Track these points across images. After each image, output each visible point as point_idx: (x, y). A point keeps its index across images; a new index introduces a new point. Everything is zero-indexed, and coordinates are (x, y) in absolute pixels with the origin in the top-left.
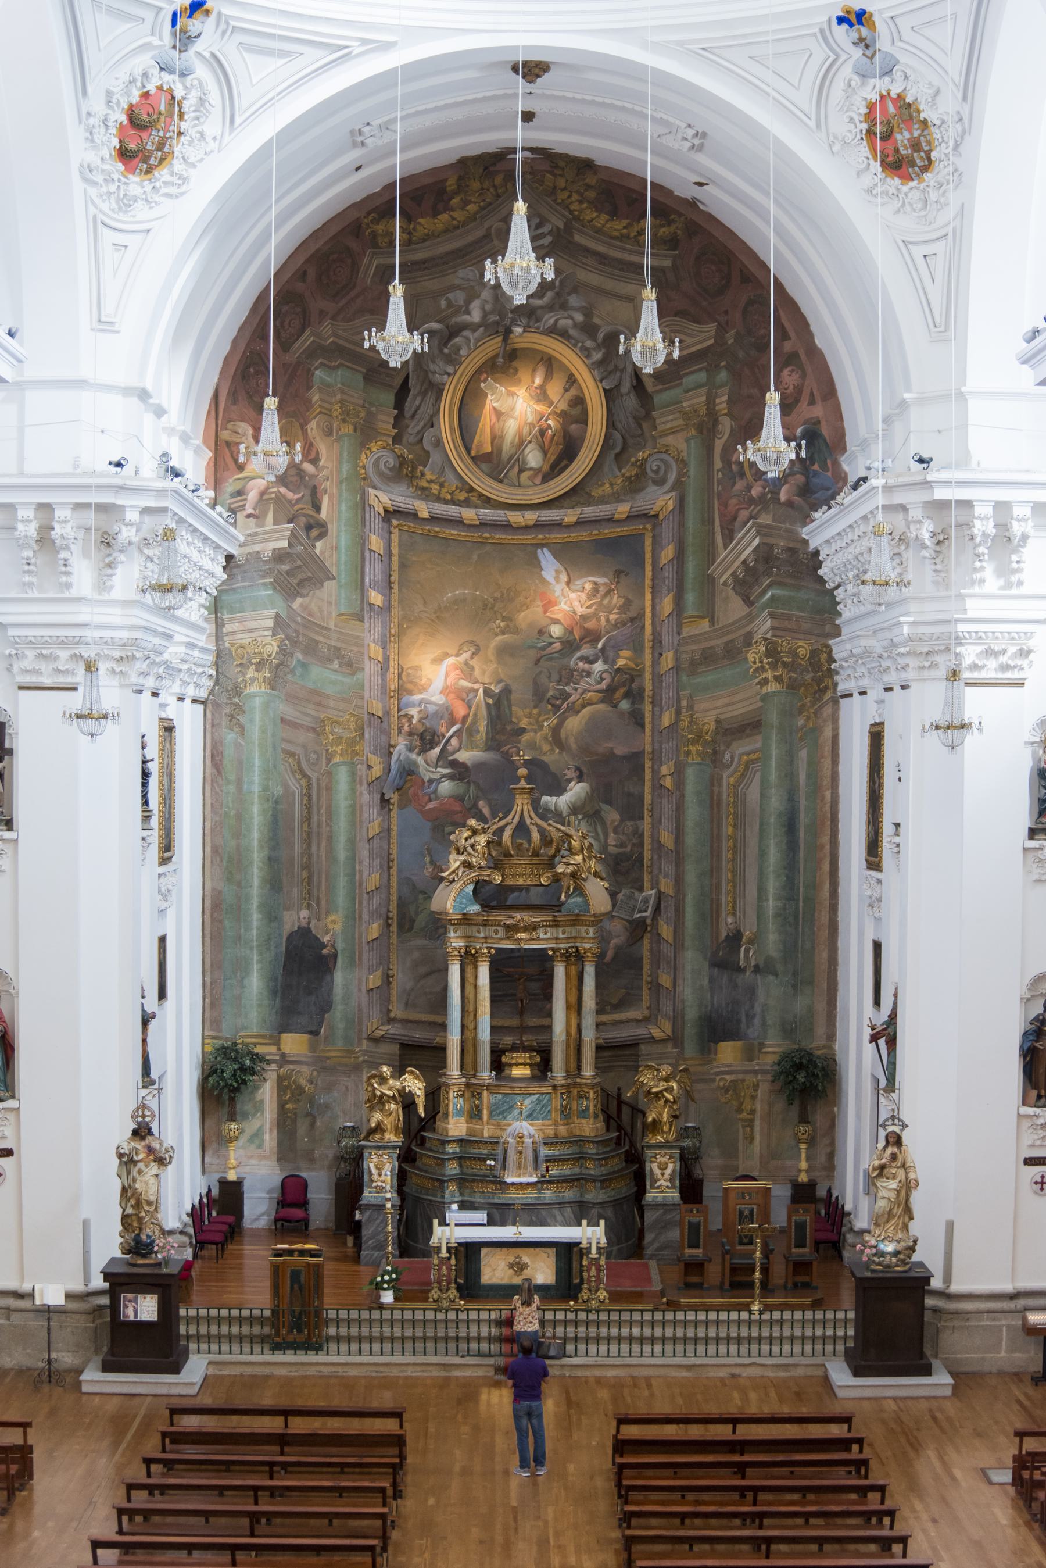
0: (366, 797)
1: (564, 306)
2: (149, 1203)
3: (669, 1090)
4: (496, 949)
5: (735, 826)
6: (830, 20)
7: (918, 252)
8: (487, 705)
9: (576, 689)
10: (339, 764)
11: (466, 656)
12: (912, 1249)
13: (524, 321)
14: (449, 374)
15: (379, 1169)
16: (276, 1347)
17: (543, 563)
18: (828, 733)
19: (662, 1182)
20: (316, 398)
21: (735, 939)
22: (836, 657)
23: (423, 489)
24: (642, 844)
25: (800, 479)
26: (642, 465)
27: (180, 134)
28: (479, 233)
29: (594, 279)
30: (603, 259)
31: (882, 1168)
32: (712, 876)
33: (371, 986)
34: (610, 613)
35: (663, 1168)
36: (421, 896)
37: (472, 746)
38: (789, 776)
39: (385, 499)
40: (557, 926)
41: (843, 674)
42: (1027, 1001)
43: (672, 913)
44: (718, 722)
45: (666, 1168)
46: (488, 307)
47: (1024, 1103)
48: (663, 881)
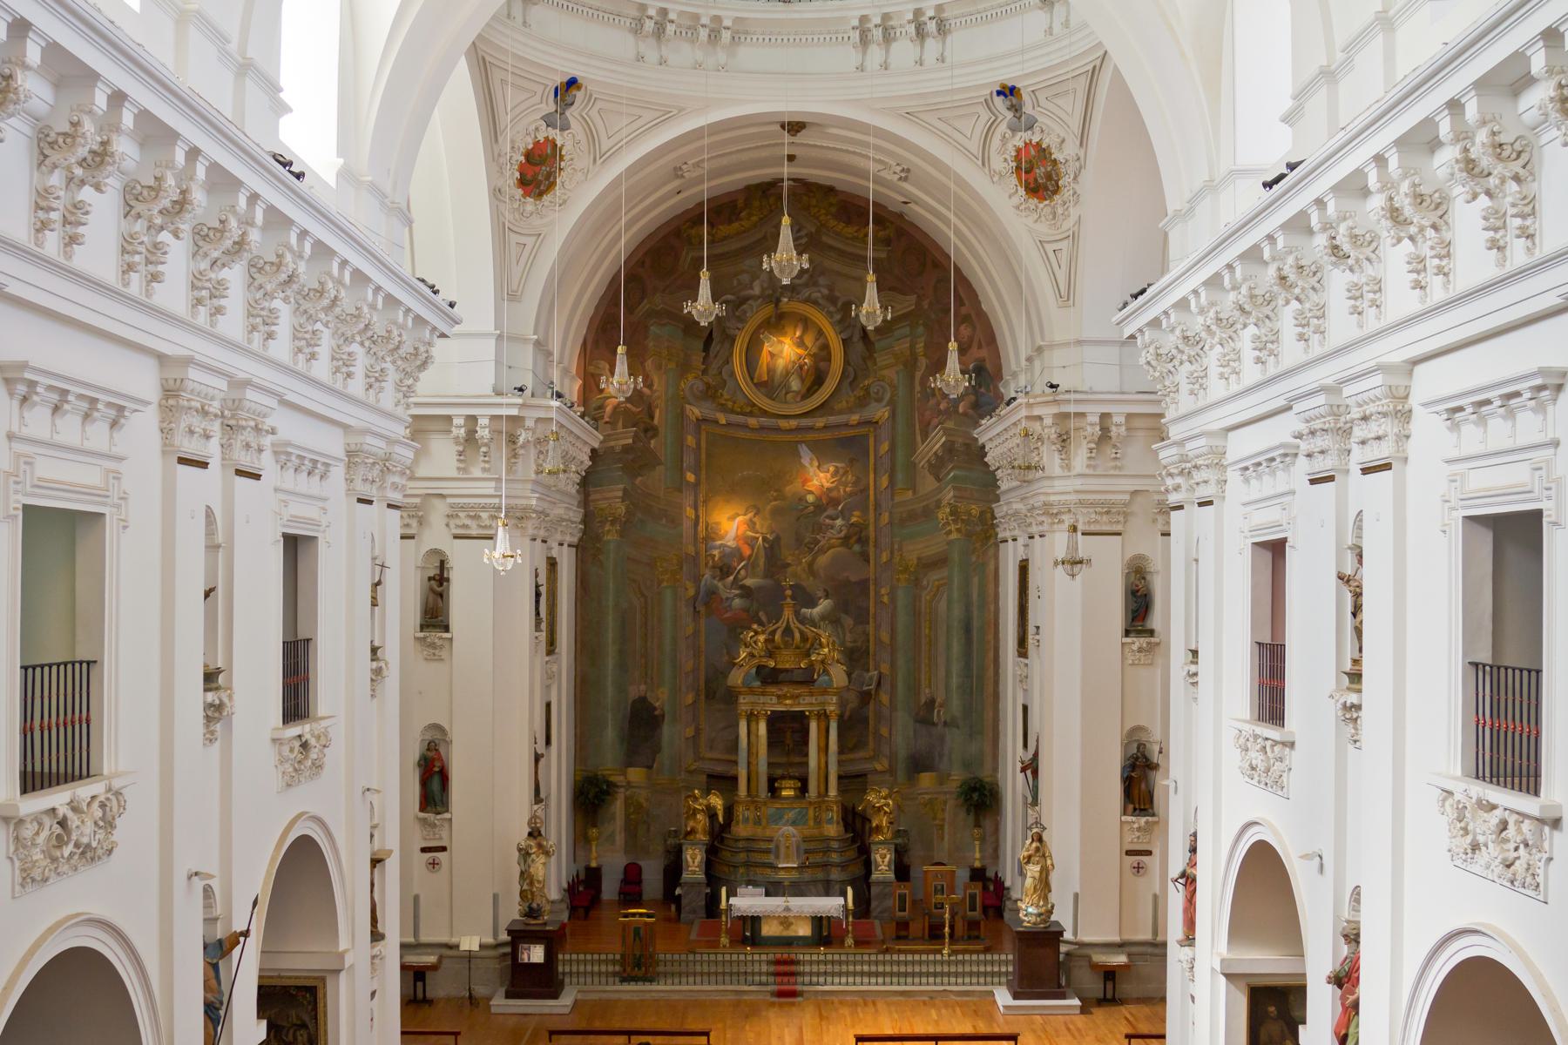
1: (815, 284)
2: (539, 882)
5: (930, 628)
6: (991, 93)
7: (1050, 248)
8: (765, 548)
11: (750, 515)
12: (1050, 912)
13: (789, 294)
14: (739, 329)
15: (693, 860)
16: (625, 979)
17: (802, 454)
18: (992, 567)
20: (651, 344)
21: (931, 703)
22: (997, 516)
23: (722, 405)
24: (868, 641)
25: (972, 398)
26: (867, 389)
27: (560, 169)
28: (759, 236)
29: (836, 266)
30: (842, 253)
31: (1029, 857)
33: (687, 736)
34: (846, 486)
35: (883, 857)
37: (754, 576)
38: (967, 596)
39: (696, 411)
41: (1002, 527)
42: (1126, 747)
44: (919, 559)
46: (765, 285)
47: (1125, 813)
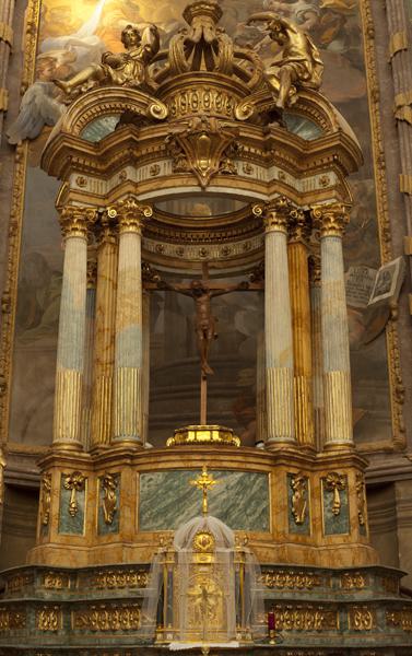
4: (152, 202)
24: (374, 211)
40: (267, 163)
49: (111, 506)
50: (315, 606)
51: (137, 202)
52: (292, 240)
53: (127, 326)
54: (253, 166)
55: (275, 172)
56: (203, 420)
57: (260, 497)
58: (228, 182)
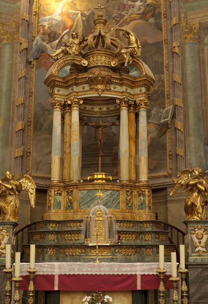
0: (19, 59)
3: (201, 184)
8: (83, 20)
9: (127, 13)
10: (5, 44)
19: (200, 248)
24: (164, 87)
32: (202, 98)
36: (46, 112)
40: (121, 85)
43: (182, 117)
44: (200, 24)
45: (202, 238)
48: (176, 99)
49: (70, 201)
50: (133, 233)
51: (78, 99)
52: (130, 111)
53: (75, 142)
54: (117, 86)
55: (124, 88)
56: (100, 170)
57: (116, 199)
58: (108, 93)
